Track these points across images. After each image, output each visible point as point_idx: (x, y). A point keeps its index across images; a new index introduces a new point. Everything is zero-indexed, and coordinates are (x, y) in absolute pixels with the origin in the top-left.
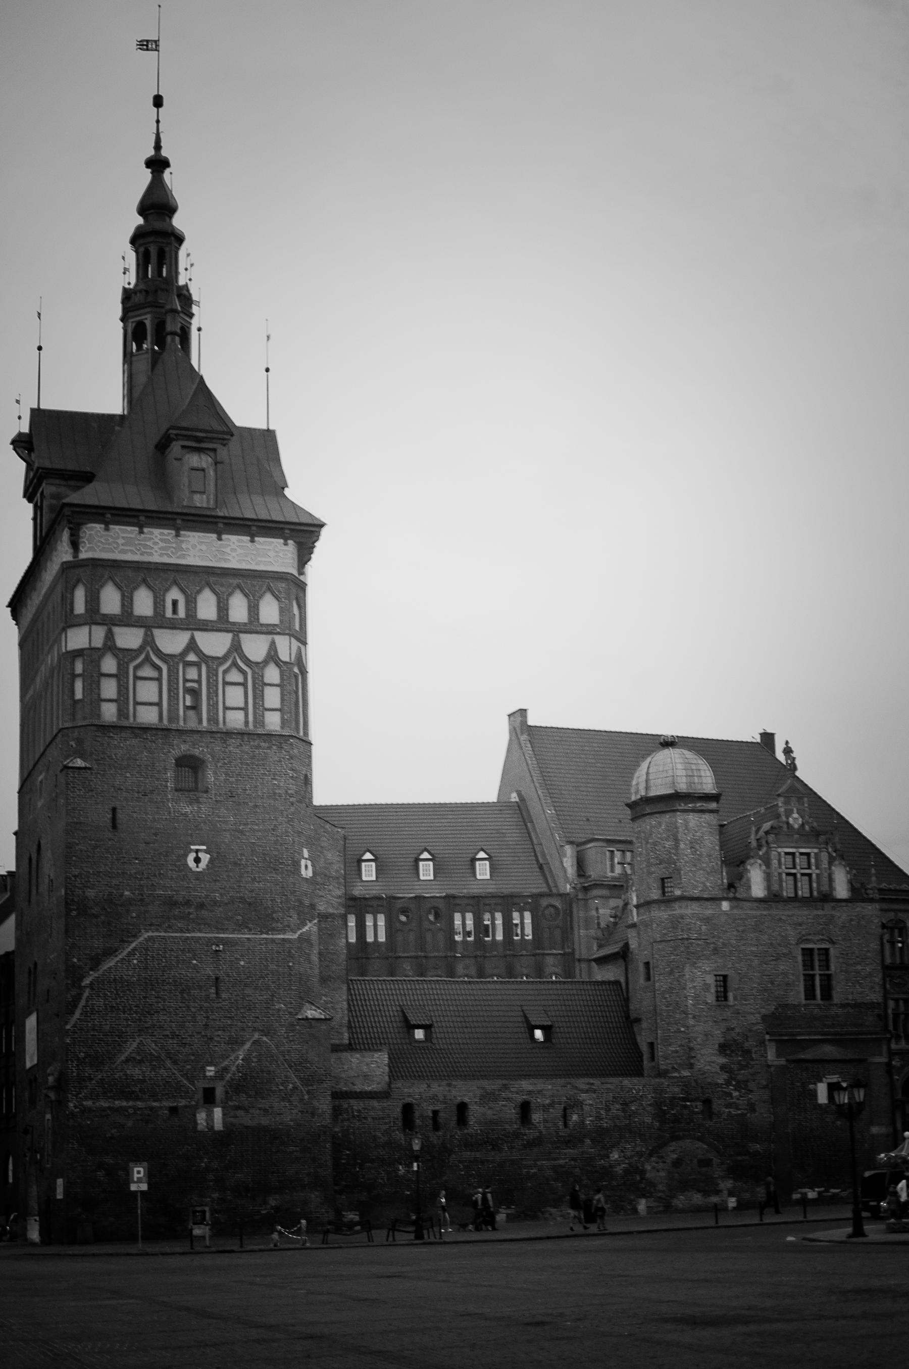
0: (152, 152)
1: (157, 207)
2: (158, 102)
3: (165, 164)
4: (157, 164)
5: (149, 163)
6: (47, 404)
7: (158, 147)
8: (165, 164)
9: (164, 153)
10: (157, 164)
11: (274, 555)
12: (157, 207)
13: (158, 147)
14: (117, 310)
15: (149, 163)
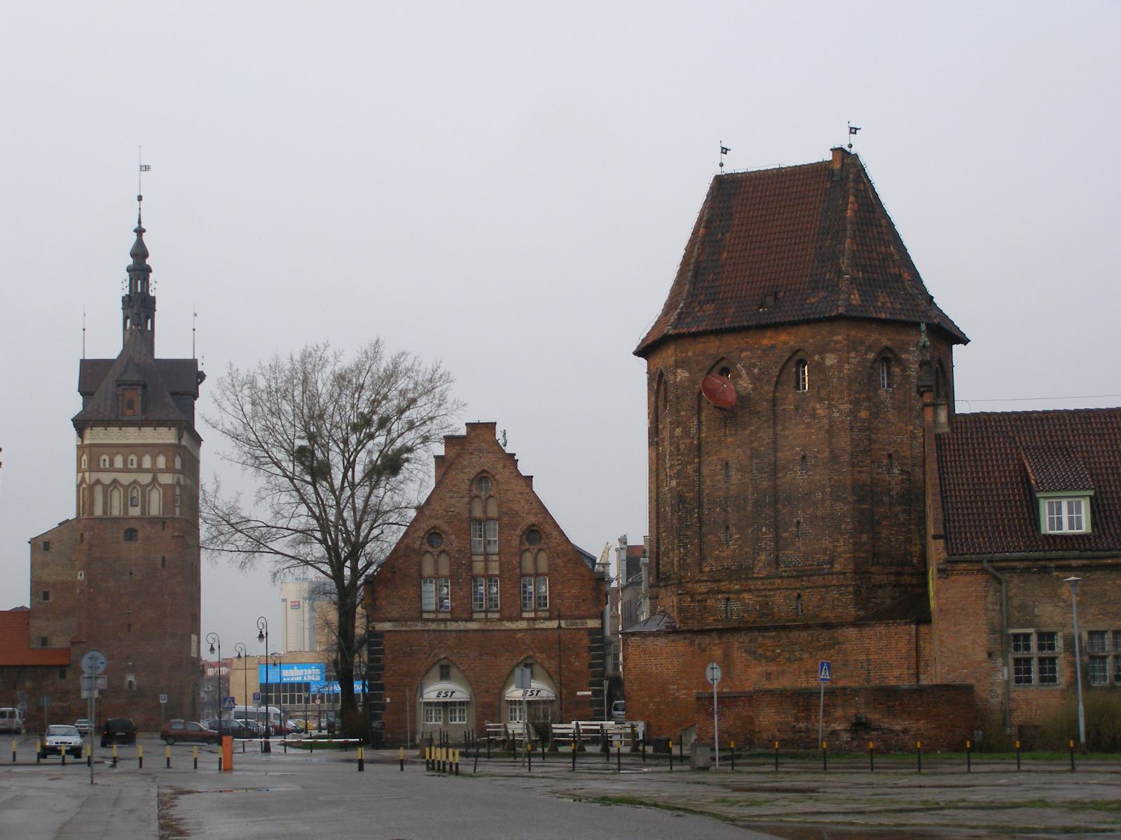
0: (136, 225)
1: (140, 253)
2: (140, 198)
3: (144, 231)
4: (140, 231)
5: (135, 231)
6: (90, 356)
7: (140, 222)
8: (144, 231)
9: (143, 226)
10: (140, 231)
11: (166, 436)
12: (140, 253)
13: (140, 222)
14: (120, 305)
15: (135, 231)
